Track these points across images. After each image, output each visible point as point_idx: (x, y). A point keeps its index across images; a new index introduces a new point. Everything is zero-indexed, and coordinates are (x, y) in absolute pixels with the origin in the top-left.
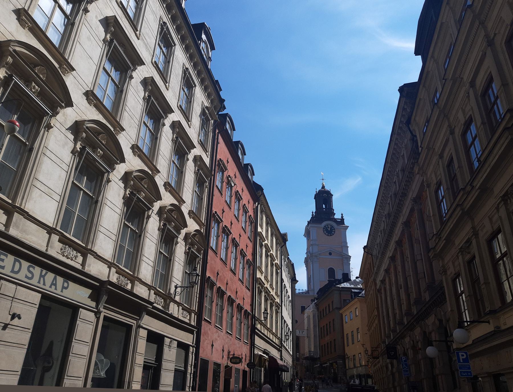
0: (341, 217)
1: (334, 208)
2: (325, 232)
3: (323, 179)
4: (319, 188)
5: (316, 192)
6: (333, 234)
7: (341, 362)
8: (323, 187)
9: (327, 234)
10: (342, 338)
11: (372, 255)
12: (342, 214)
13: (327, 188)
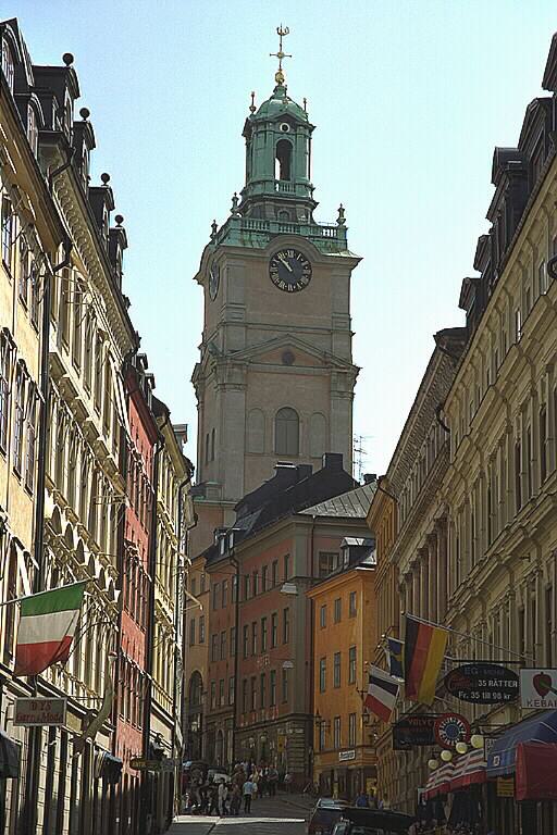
0: (341, 220)
1: (313, 181)
2: (276, 277)
3: (281, 56)
4: (265, 93)
5: (253, 108)
6: (304, 286)
7: (301, 731)
8: (280, 89)
9: (282, 285)
10: (307, 663)
11: (396, 501)
12: (341, 211)
13: (295, 94)
